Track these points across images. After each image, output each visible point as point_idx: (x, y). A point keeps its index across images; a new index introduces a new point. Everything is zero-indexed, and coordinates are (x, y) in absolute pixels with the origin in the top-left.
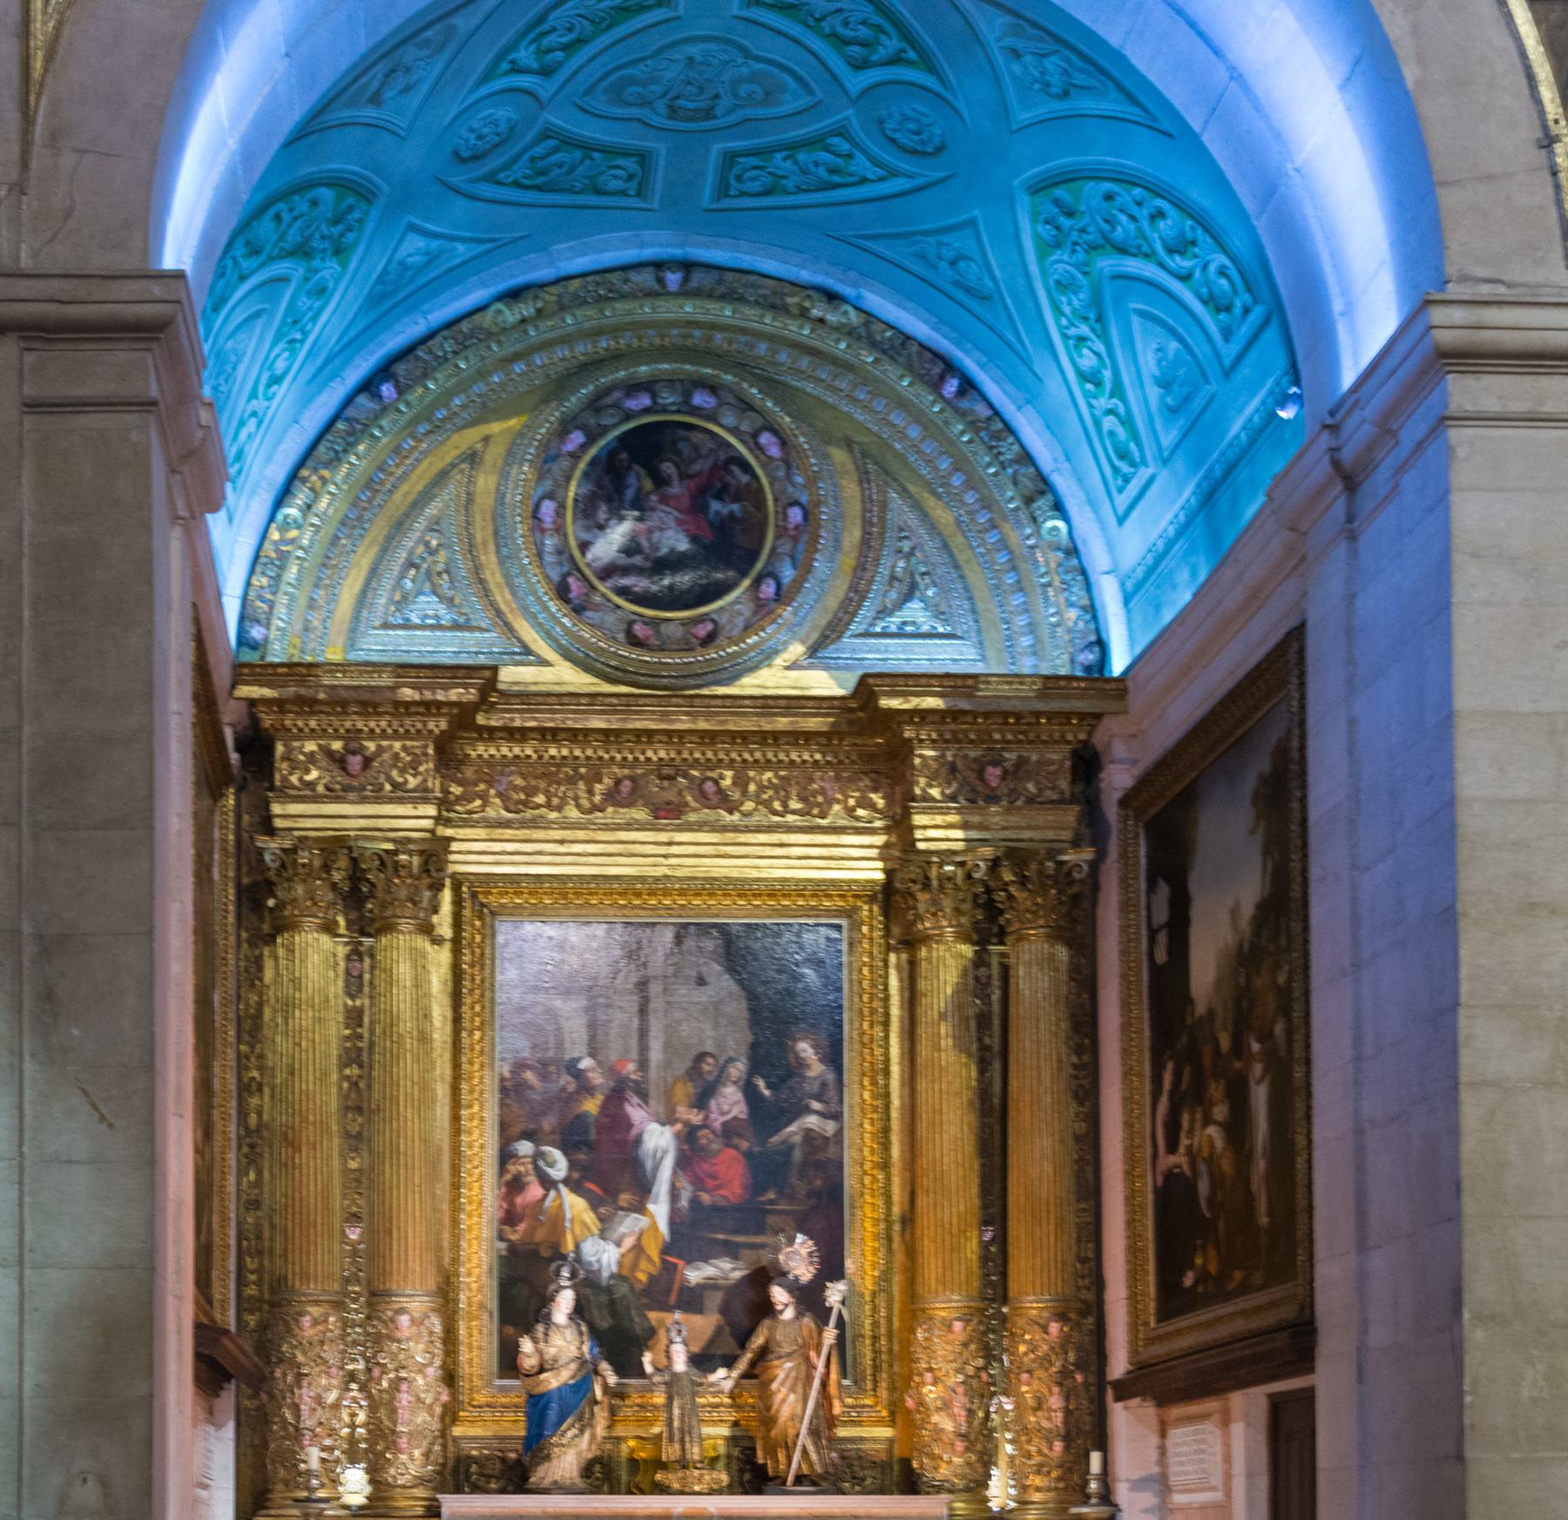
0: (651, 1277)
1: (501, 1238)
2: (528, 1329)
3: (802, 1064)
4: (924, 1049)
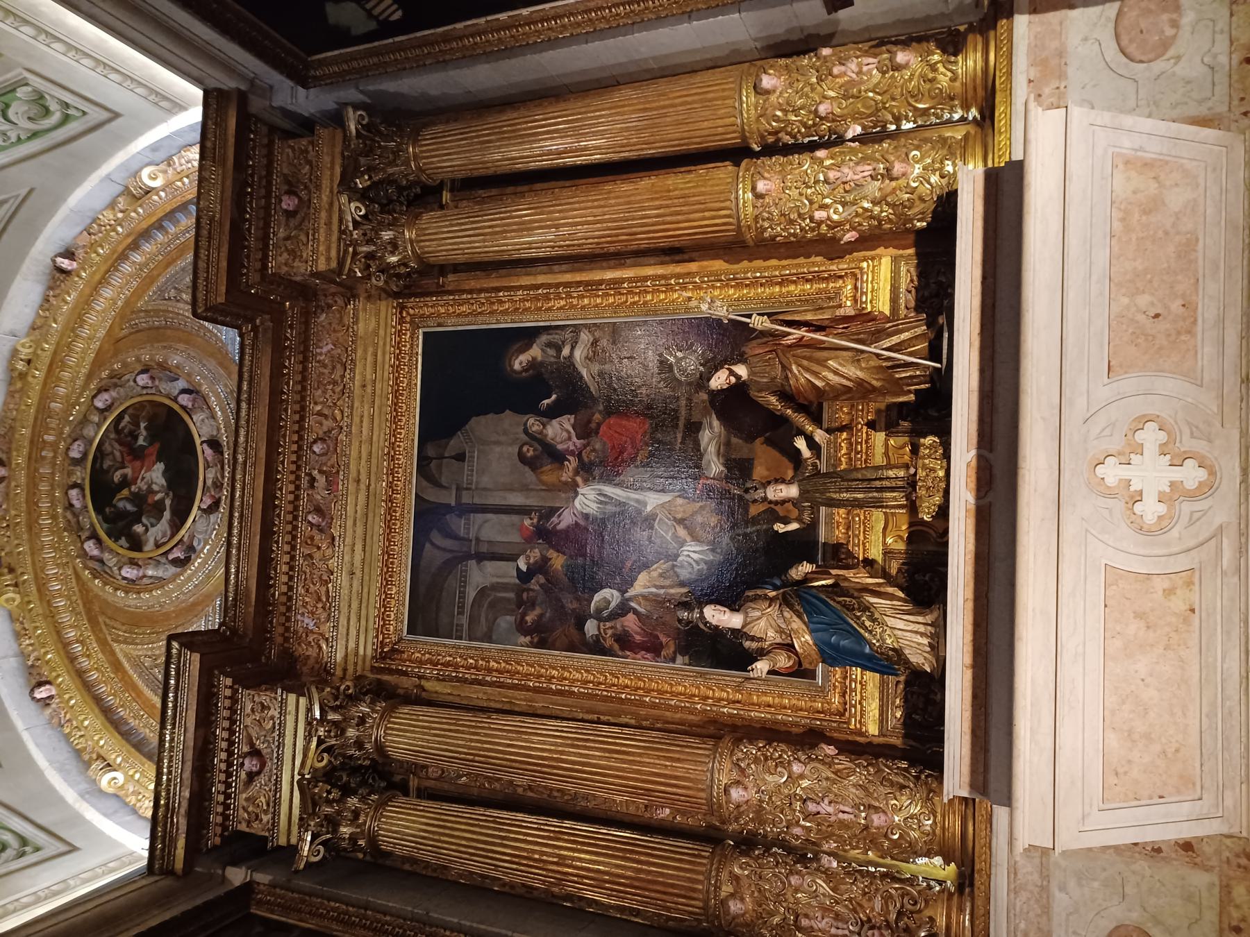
1: (673, 660)
3: (533, 364)
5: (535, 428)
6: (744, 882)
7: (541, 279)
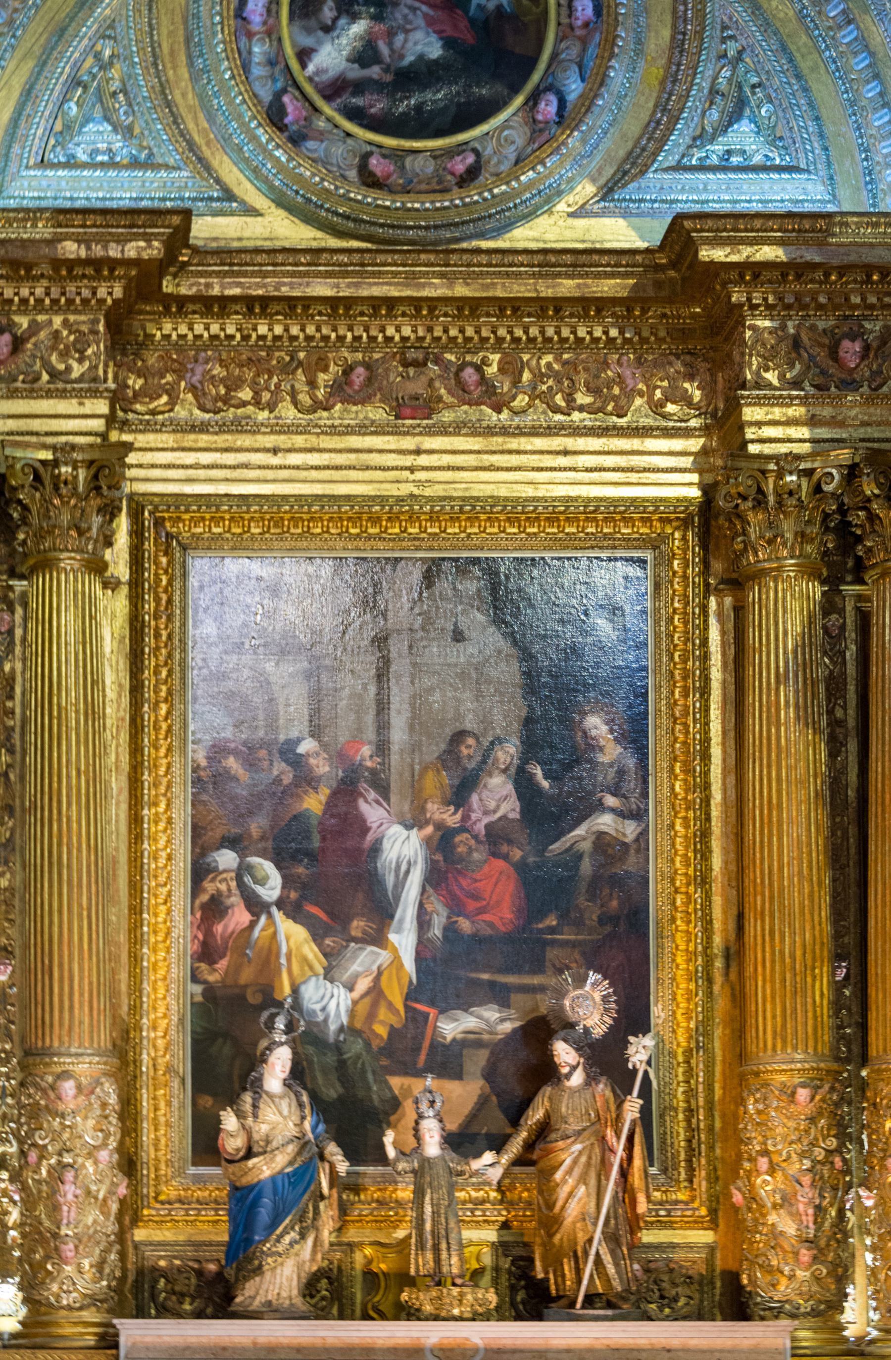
0: (393, 1031)
1: (195, 979)
2: (232, 1100)
3: (592, 746)
4: (755, 724)
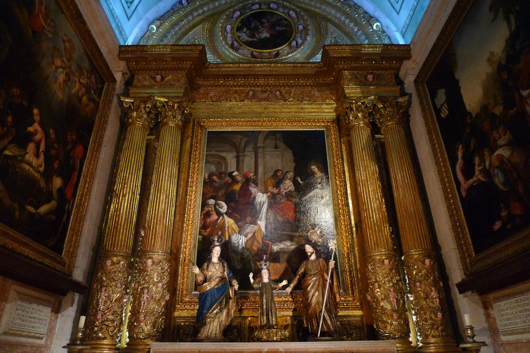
5: (289, 176)
6: (117, 266)
7: (347, 175)
